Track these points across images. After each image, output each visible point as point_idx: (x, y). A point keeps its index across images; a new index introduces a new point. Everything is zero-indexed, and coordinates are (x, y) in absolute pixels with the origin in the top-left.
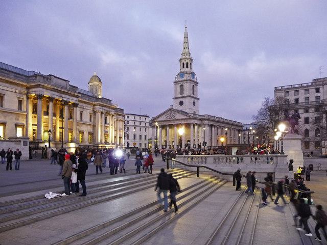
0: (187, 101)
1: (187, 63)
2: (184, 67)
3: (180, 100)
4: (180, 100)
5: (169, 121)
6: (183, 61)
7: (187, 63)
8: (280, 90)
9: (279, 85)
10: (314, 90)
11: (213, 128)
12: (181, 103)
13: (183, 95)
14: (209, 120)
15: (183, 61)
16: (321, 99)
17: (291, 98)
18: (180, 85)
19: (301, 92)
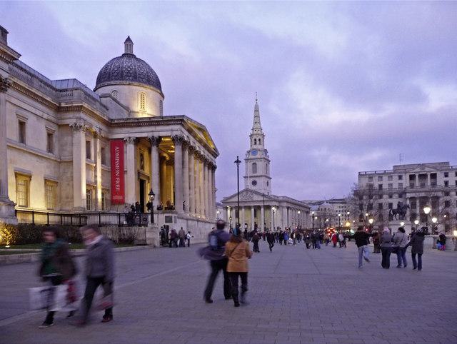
0: (261, 181)
1: (259, 140)
2: (256, 143)
3: (253, 179)
4: (253, 179)
5: (246, 202)
6: (254, 137)
7: (259, 140)
8: (363, 175)
9: (363, 170)
10: (397, 177)
11: (289, 211)
12: (254, 183)
13: (255, 175)
14: (288, 202)
15: (254, 137)
16: (404, 186)
17: (376, 184)
18: (251, 163)
19: (385, 178)
